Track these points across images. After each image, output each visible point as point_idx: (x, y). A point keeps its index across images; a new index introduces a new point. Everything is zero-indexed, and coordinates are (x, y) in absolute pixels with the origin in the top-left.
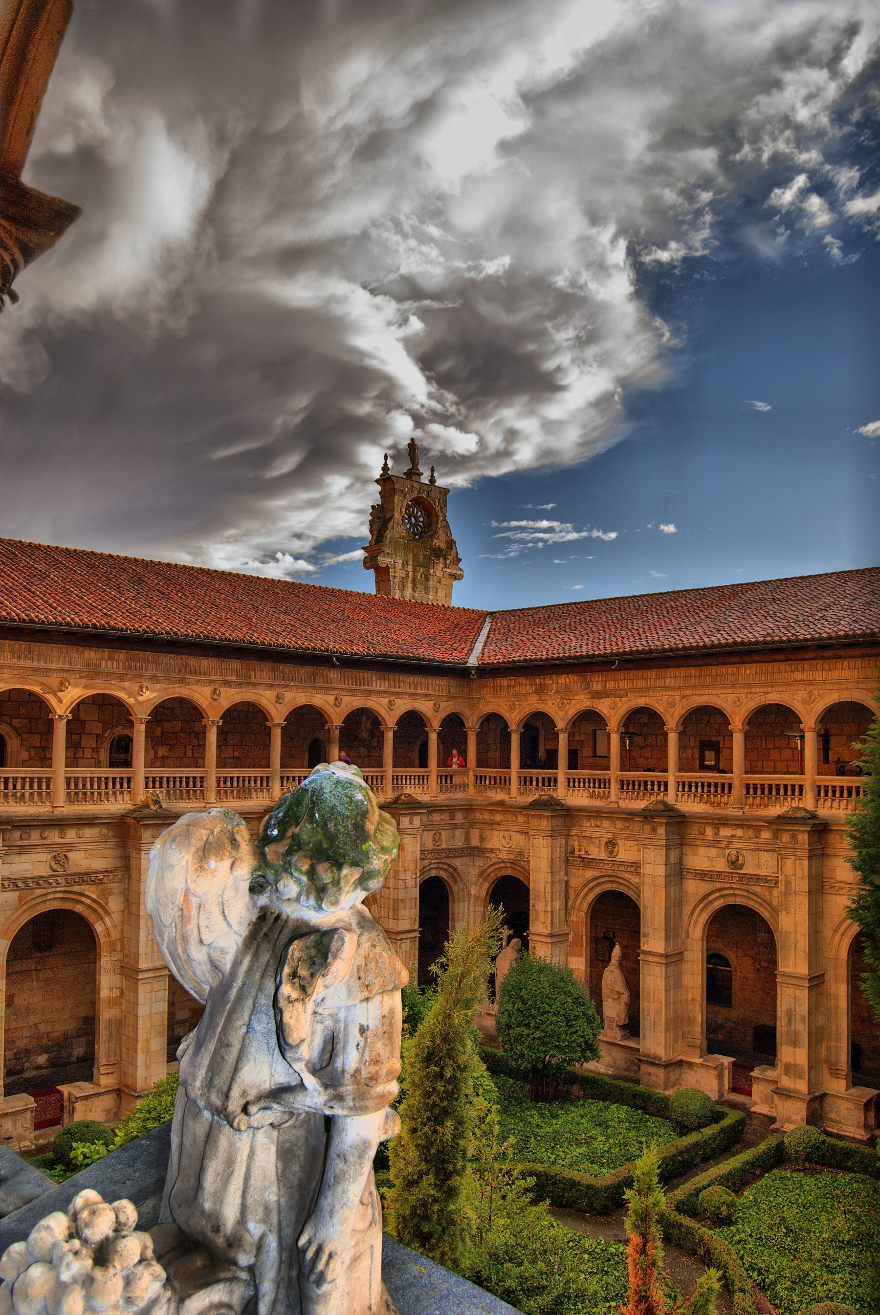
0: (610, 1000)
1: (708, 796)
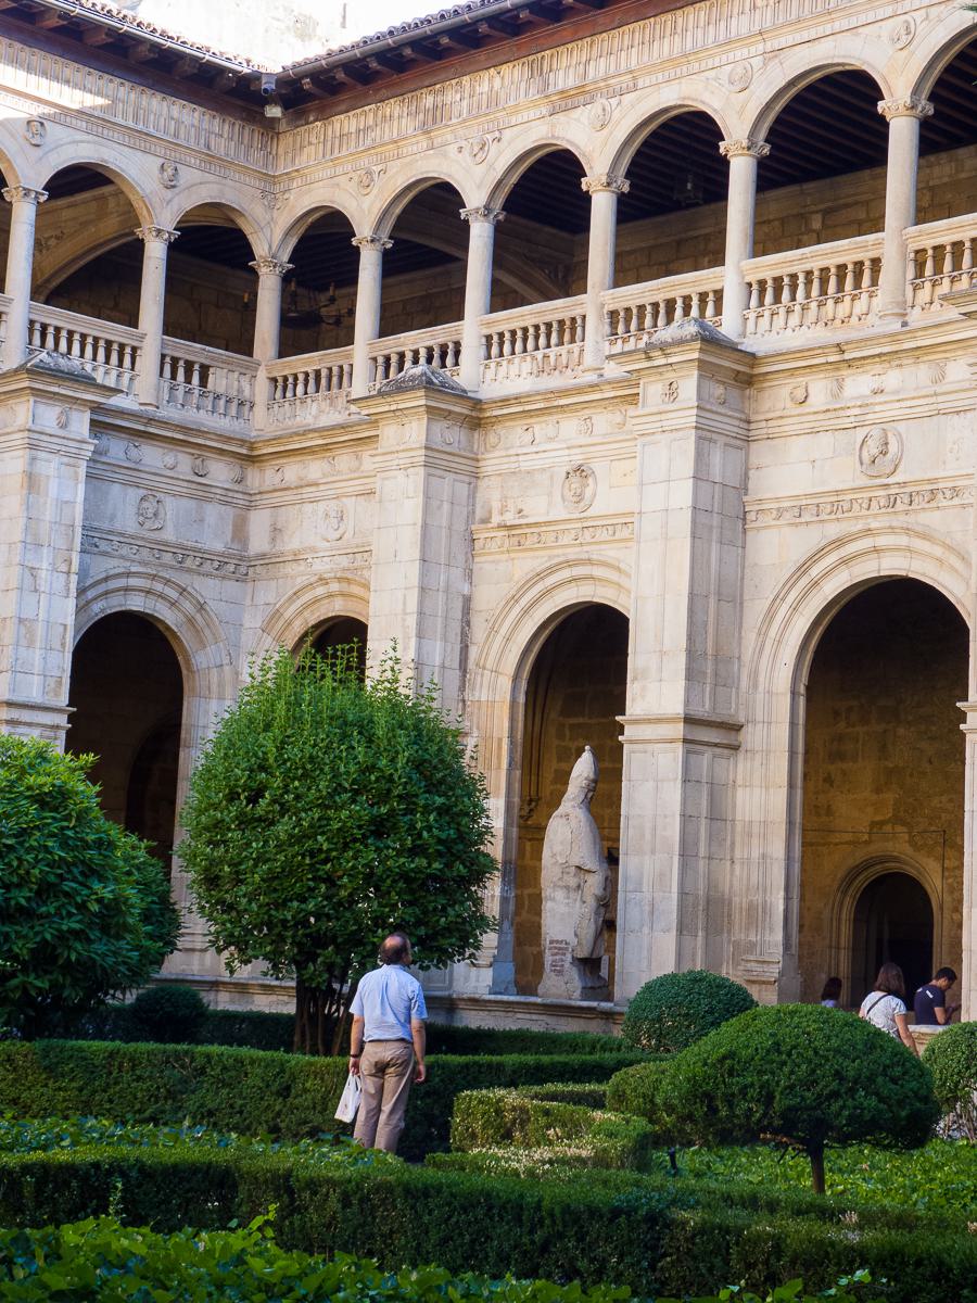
0: (560, 895)
1: (821, 305)
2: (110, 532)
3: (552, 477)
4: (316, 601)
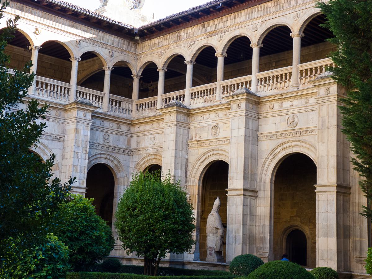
0: (211, 235)
1: (276, 84)
2: (96, 143)
3: (208, 128)
4: (148, 160)
